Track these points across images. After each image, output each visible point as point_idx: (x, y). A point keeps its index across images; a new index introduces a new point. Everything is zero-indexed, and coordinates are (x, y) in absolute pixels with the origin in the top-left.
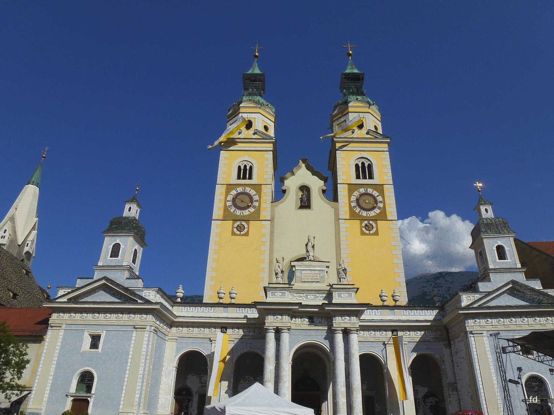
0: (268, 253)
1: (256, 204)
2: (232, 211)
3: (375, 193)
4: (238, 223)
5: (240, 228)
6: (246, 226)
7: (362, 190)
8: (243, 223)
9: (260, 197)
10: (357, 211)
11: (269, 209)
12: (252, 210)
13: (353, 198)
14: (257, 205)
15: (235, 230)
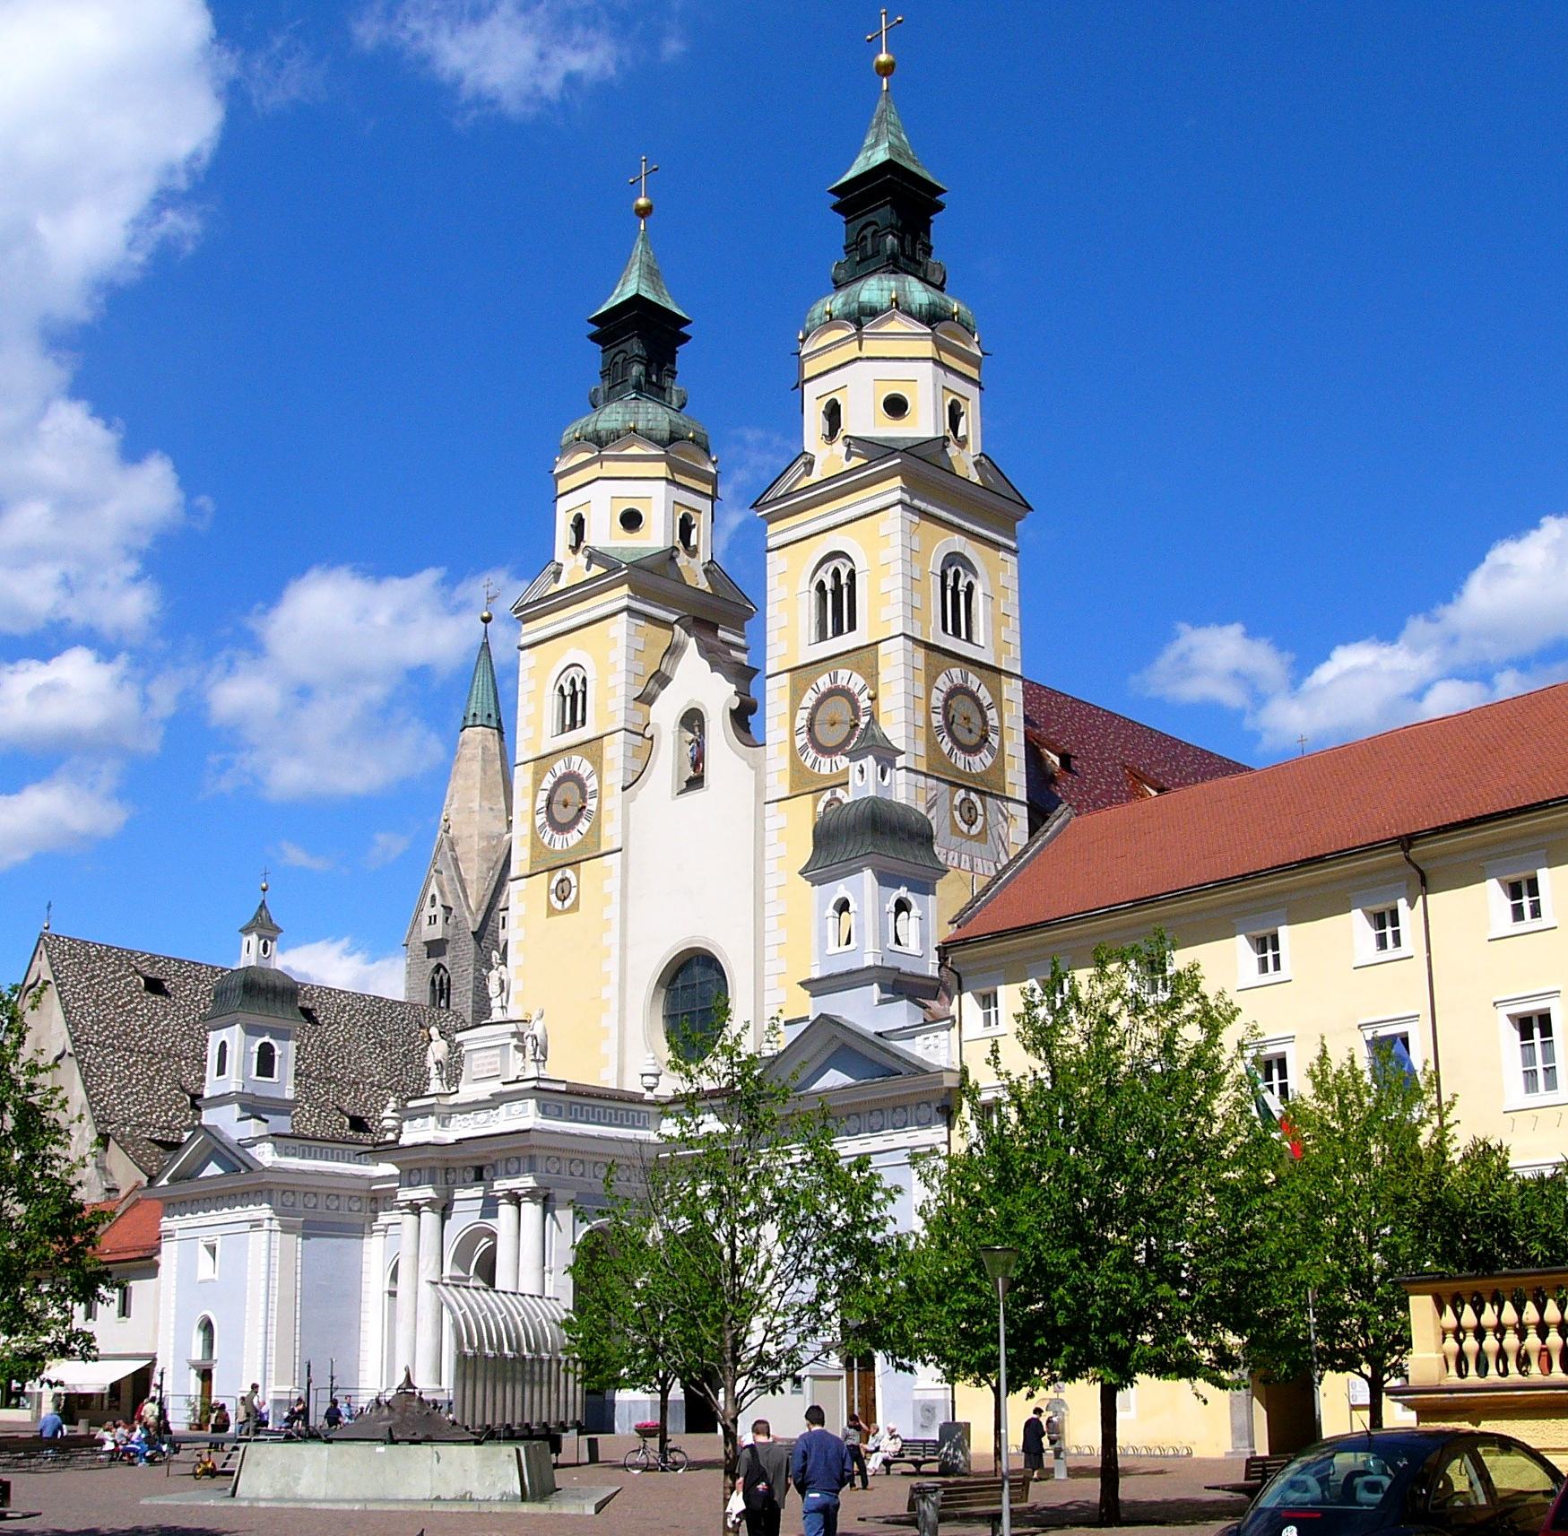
0: (616, 951)
1: (592, 804)
2: (546, 841)
3: (856, 683)
4: (558, 875)
5: (562, 891)
6: (574, 883)
7: (824, 683)
8: (569, 873)
9: (600, 782)
10: (808, 763)
11: (618, 815)
12: (584, 826)
13: (802, 718)
14: (594, 808)
15: (553, 897)
